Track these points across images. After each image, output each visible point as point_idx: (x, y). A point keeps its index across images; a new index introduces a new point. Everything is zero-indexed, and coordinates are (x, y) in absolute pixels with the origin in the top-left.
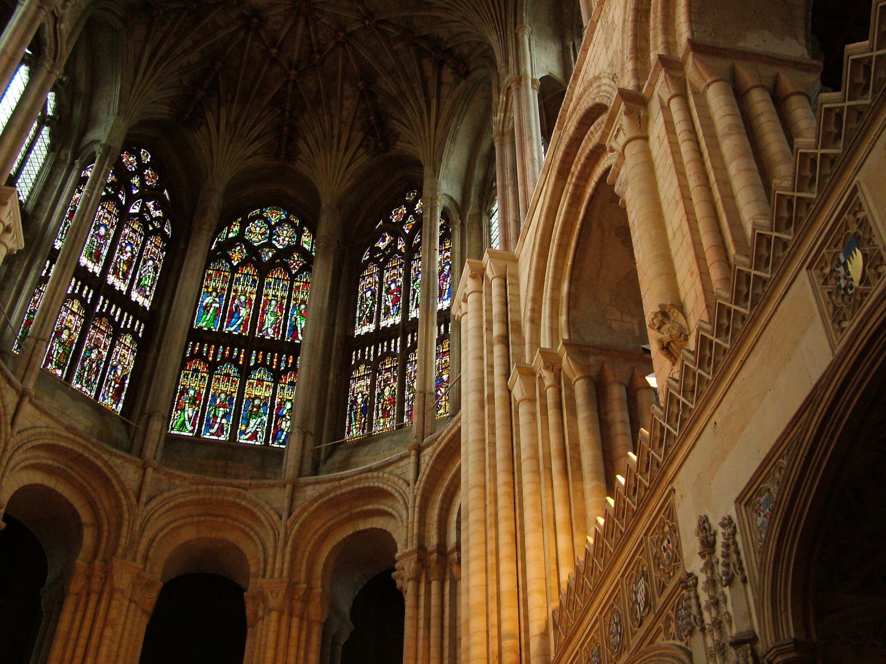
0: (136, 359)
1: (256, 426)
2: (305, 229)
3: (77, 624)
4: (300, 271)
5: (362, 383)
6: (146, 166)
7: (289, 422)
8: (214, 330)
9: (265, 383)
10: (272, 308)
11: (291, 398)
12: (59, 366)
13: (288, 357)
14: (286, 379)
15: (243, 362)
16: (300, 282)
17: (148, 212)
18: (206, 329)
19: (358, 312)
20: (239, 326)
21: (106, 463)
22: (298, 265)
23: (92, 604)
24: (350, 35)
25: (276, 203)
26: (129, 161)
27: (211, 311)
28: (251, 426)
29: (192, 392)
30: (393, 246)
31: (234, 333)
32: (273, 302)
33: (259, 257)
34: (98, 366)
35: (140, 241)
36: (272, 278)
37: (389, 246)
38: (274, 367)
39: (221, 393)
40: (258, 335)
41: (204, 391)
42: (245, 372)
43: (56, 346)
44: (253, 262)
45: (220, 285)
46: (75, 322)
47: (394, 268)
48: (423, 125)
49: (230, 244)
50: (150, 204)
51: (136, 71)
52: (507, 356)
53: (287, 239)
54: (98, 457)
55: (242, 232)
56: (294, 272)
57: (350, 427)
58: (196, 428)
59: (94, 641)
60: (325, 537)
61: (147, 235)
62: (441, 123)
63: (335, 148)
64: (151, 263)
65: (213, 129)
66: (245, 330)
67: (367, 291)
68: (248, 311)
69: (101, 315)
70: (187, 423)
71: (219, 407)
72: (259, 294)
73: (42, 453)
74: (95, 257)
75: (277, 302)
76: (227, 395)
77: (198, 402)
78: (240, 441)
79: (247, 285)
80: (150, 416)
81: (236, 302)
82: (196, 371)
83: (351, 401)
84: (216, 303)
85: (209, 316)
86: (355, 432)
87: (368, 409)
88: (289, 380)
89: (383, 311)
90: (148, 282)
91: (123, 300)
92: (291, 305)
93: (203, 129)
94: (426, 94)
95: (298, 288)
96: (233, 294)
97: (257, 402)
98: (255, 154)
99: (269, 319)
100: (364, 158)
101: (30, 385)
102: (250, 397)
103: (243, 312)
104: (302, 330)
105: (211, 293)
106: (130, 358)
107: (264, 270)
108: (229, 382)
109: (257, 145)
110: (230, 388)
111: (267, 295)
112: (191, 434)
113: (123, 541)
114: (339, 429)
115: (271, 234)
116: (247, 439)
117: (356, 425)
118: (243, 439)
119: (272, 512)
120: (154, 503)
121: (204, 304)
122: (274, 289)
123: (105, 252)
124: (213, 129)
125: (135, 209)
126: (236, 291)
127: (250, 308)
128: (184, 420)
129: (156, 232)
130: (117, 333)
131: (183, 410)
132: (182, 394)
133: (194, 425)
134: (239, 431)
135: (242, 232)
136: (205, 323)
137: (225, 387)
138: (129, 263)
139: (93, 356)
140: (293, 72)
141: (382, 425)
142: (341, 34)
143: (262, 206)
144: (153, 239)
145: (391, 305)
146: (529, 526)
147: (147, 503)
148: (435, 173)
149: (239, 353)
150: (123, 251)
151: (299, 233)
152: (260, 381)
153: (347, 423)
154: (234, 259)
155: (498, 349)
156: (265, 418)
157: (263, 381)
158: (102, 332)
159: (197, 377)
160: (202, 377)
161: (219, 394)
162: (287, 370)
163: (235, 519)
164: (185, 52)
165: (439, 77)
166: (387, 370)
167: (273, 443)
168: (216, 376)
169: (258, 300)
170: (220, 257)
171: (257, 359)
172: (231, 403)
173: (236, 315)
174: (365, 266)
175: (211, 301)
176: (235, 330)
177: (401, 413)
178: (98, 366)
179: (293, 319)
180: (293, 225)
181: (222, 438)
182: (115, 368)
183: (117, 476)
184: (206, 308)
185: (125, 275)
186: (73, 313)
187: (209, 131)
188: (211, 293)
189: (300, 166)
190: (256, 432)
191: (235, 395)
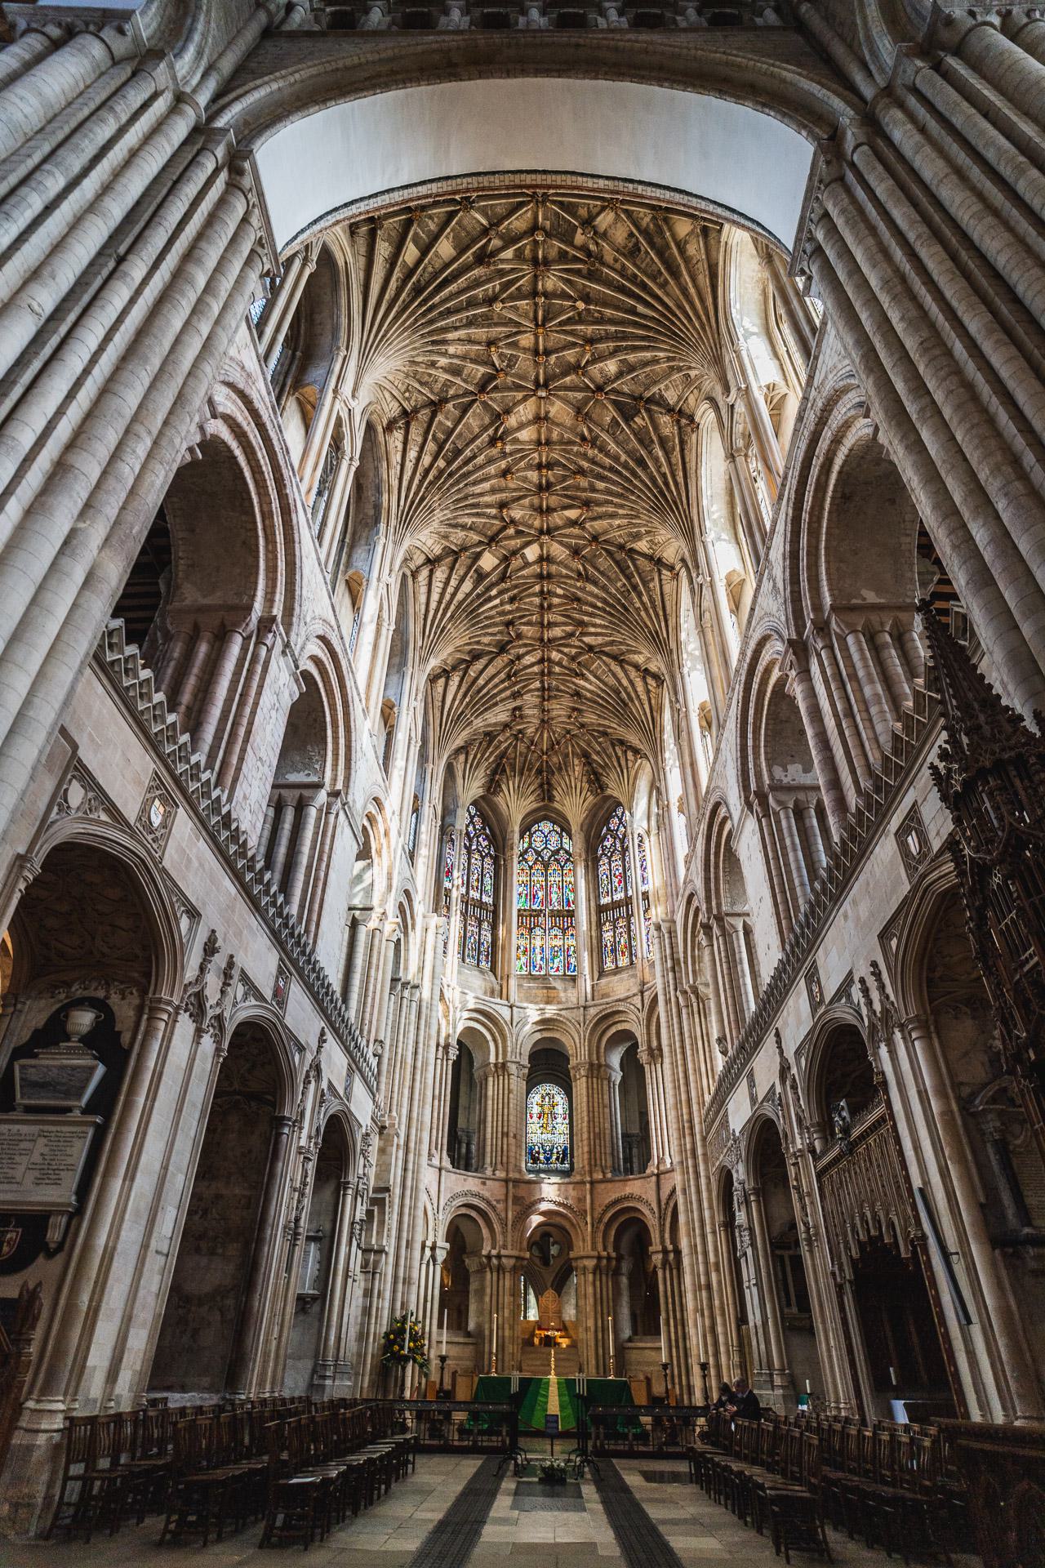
25: (545, 818)
49: (526, 852)
52: (675, 978)
60: (604, 1032)
87: (614, 951)
91: (480, 904)
99: (554, 897)
103: (540, 894)
107: (546, 866)
114: (601, 962)
130: (480, 922)
141: (623, 961)
143: (537, 822)
146: (691, 1072)
151: (561, 837)
155: (671, 975)
177: (631, 955)
189: (556, 805)
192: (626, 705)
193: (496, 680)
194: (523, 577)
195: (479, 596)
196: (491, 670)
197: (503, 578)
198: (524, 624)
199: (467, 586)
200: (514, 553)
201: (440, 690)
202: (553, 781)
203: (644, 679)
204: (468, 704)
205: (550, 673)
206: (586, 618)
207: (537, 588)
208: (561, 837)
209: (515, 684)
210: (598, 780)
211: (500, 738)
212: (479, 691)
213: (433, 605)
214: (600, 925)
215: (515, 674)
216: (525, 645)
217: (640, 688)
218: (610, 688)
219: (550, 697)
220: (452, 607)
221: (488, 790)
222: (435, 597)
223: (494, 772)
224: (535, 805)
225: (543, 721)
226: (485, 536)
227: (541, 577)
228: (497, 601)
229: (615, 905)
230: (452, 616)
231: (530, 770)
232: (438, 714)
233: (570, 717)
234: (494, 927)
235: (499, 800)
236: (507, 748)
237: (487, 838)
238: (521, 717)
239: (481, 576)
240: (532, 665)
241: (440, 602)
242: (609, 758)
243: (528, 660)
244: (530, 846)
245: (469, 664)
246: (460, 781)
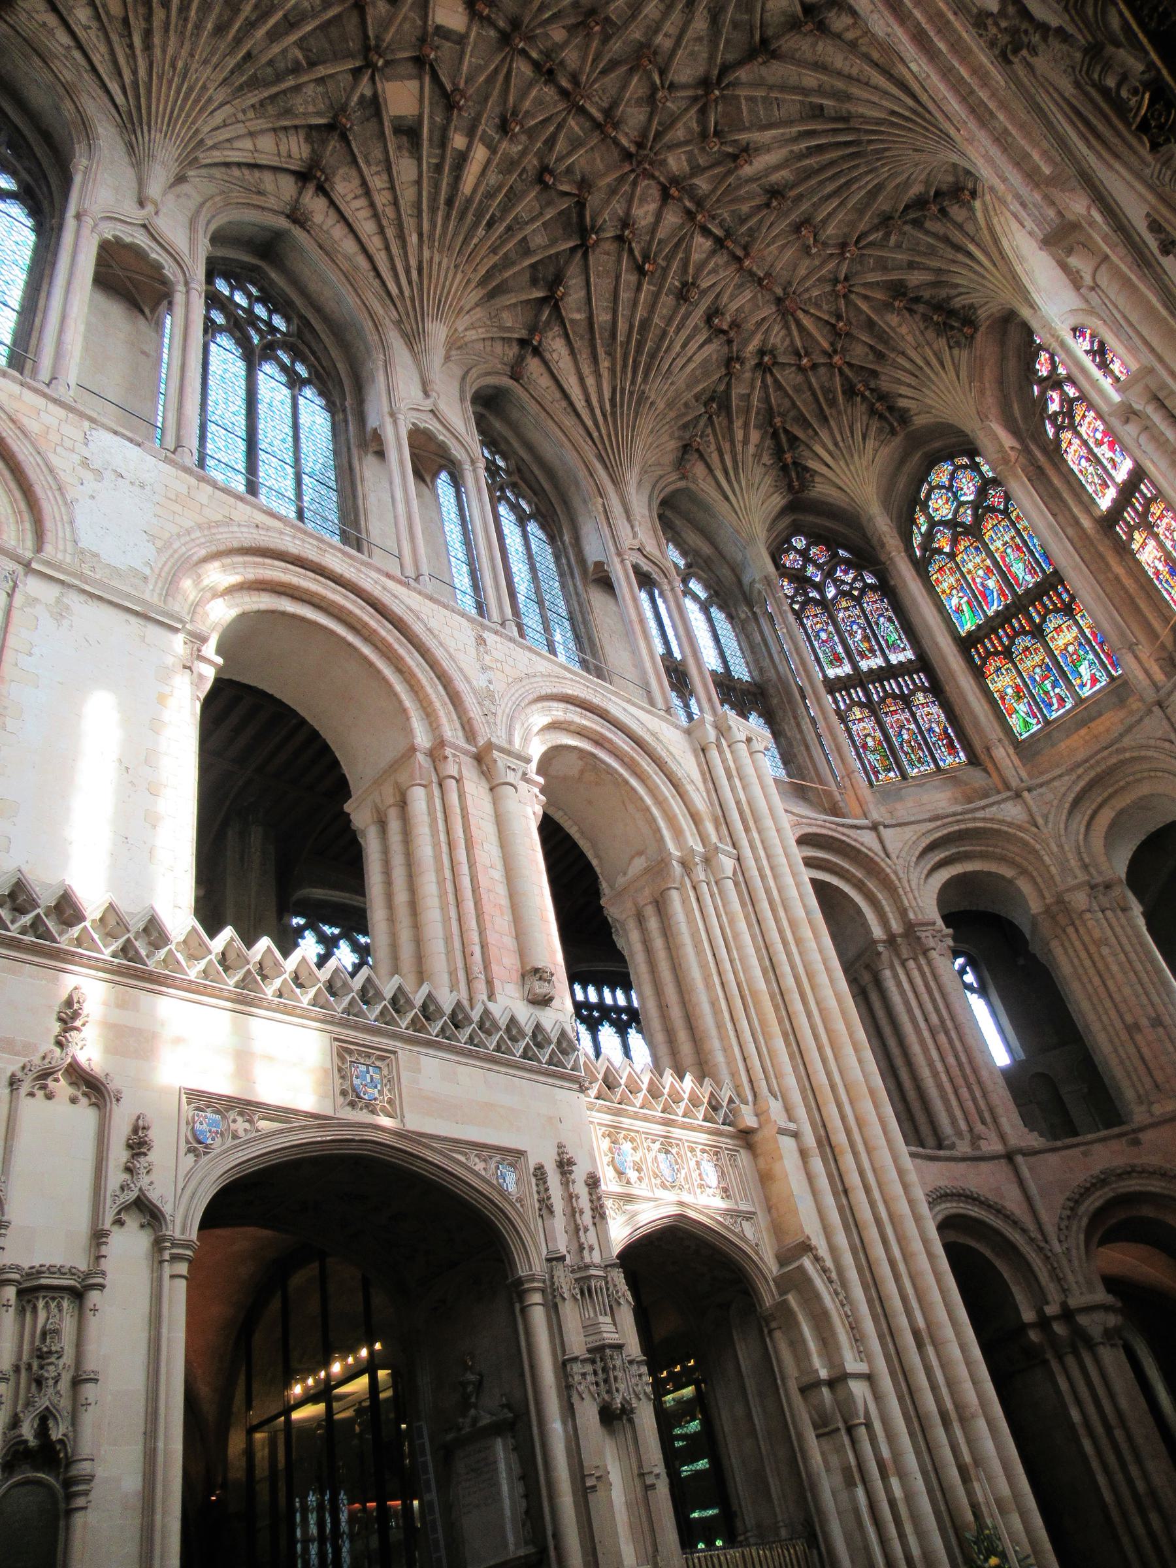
0: (941, 706)
2: (977, 459)
3: (1076, 961)
5: (1149, 548)
6: (807, 549)
12: (889, 770)
17: (843, 582)
19: (1088, 487)
21: (984, 819)
23: (1074, 936)
24: (846, 279)
25: (932, 462)
26: (791, 560)
29: (1010, 691)
30: (1065, 399)
32: (1009, 551)
33: (962, 525)
34: (916, 741)
35: (858, 612)
37: (1061, 402)
40: (1020, 591)
41: (1018, 681)
42: (1038, 632)
43: (872, 757)
44: (961, 534)
45: (952, 580)
46: (869, 725)
47: (1084, 416)
48: (984, 277)
49: (929, 536)
50: (838, 574)
51: (727, 498)
54: (975, 819)
55: (930, 518)
59: (1100, 965)
61: (858, 600)
62: (996, 256)
63: (932, 376)
64: (882, 620)
65: (823, 470)
69: (882, 700)
72: (990, 555)
73: (930, 855)
74: (837, 660)
80: (988, 749)
81: (978, 580)
82: (998, 669)
89: (1109, 467)
90: (895, 636)
91: (890, 672)
93: (817, 479)
94: (958, 248)
95: (1018, 517)
96: (969, 577)
97: (1071, 649)
98: (876, 451)
99: (1018, 569)
100: (965, 354)
101: (875, 816)
103: (991, 583)
106: (935, 710)
109: (871, 443)
110: (1037, 659)
113: (1053, 870)
115: (955, 494)
118: (1086, 692)
119: (1160, 743)
120: (1051, 818)
123: (840, 649)
124: (823, 470)
125: (831, 592)
126: (969, 572)
129: (863, 592)
130: (906, 701)
131: (1016, 711)
132: (1003, 698)
133: (1035, 716)
135: (930, 518)
137: (1031, 663)
138: (866, 638)
139: (906, 737)
140: (836, 359)
142: (839, 287)
143: (923, 477)
144: (866, 599)
145: (1110, 454)
147: (1046, 822)
148: (1032, 306)
149: (1019, 621)
150: (852, 634)
151: (976, 467)
152: (1058, 629)
156: (1091, 656)
158: (895, 712)
163: (1134, 774)
164: (746, 442)
165: (954, 223)
166: (1161, 518)
170: (931, 557)
171: (1038, 613)
172: (1049, 670)
174: (1058, 441)
178: (916, 741)
180: (965, 467)
181: (1068, 706)
182: (930, 730)
183: (1002, 822)
184: (959, 610)
185: (872, 651)
186: (861, 720)
187: (822, 475)
189: (919, 421)
192: (845, 119)
193: (625, 295)
194: (476, 70)
195: (438, 168)
196: (601, 286)
197: (448, 101)
198: (570, 154)
199: (405, 169)
200: (423, 40)
201: (545, 381)
202: (885, 385)
203: (822, 28)
204: (613, 371)
205: (699, 203)
206: (636, 33)
207: (523, 68)
209: (664, 277)
210: (952, 313)
211: (738, 390)
212: (613, 335)
213: (375, 244)
214: (1124, 550)
215: (646, 258)
216: (613, 191)
217: (839, 60)
218: (802, 119)
219: (746, 248)
220: (409, 223)
221: (790, 487)
222: (367, 228)
223: (778, 453)
224: (885, 451)
225: (779, 301)
226: (350, 55)
227: (505, 39)
228: (480, 154)
229: (1128, 490)
230: (420, 235)
231: (832, 403)
232: (569, 422)
233: (806, 250)
234: (937, 690)
235: (820, 490)
236: (766, 399)
237: (849, 564)
238: (735, 325)
239: (409, 132)
240: (659, 216)
241: (381, 231)
242: (932, 252)
243: (644, 213)
244: (933, 524)
245: (552, 302)
246: (722, 507)
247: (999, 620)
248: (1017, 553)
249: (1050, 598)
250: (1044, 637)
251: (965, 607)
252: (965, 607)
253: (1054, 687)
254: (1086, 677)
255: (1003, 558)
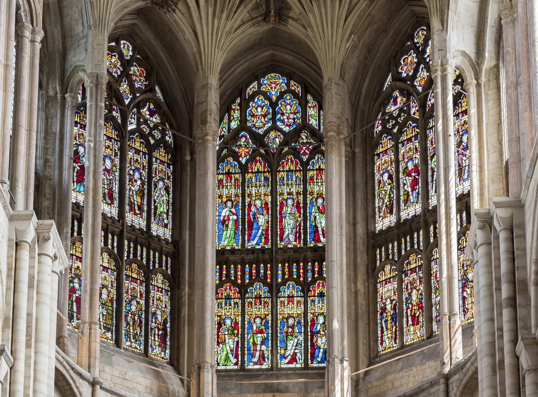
1: (294, 348)
4: (311, 157)
7: (324, 338)
8: (237, 248)
9: (295, 298)
10: (289, 209)
11: (322, 311)
13: (313, 266)
14: (315, 291)
15: (271, 279)
16: (313, 170)
18: (228, 248)
20: (260, 239)
22: (308, 149)
27: (230, 226)
28: (289, 348)
29: (228, 322)
31: (258, 247)
32: (290, 202)
36: (283, 171)
38: (302, 279)
39: (256, 317)
41: (239, 319)
44: (261, 155)
45: (233, 191)
53: (292, 116)
56: (305, 158)
57: (382, 337)
58: (240, 359)
66: (266, 243)
67: (384, 173)
68: (266, 218)
70: (230, 355)
71: (257, 333)
72: (273, 193)
75: (293, 200)
76: (262, 319)
77: (236, 332)
78: (283, 366)
79: (260, 186)
81: (253, 209)
82: (228, 298)
83: (381, 308)
84: (234, 214)
85: (229, 232)
86: (387, 343)
87: (396, 318)
88: (317, 291)
92: (308, 202)
95: (312, 178)
96: (247, 200)
97: (291, 321)
102: (283, 317)
103: (262, 220)
104: (323, 230)
105: (226, 203)
108: (261, 304)
110: (263, 311)
111: (282, 194)
112: (236, 367)
116: (288, 363)
117: (387, 334)
118: (284, 364)
121: (222, 218)
122: (288, 185)
126: (250, 195)
127: (268, 213)
128: (227, 353)
133: (236, 357)
134: (279, 355)
136: (226, 242)
151: (304, 104)
153: (379, 332)
154: (241, 156)
156: (301, 338)
157: (293, 297)
159: (230, 305)
160: (236, 303)
161: (254, 319)
162: (314, 281)
167: (312, 363)
168: (248, 300)
169: (274, 201)
170: (226, 156)
171: (284, 274)
172: (267, 328)
173: (255, 226)
175: (227, 214)
176: (257, 244)
179: (312, 219)
181: (264, 367)
188: (226, 203)
190: (295, 354)
191: (269, 318)
208: (304, 104)
244: (243, 126)
247: (251, 257)
248: (294, 210)
249: (298, 269)
250: (278, 297)
251: (231, 224)
252: (231, 224)
253: (262, 343)
254: (290, 352)
255: (282, 205)
